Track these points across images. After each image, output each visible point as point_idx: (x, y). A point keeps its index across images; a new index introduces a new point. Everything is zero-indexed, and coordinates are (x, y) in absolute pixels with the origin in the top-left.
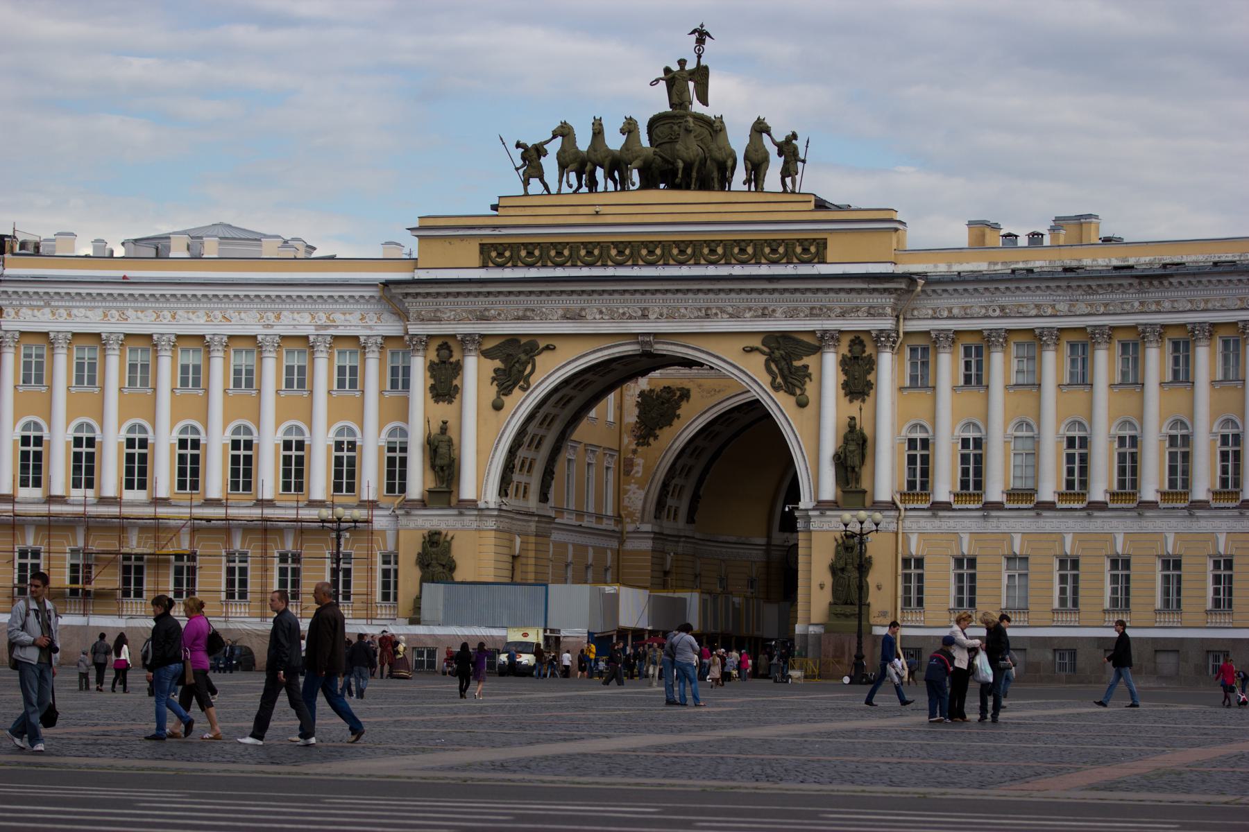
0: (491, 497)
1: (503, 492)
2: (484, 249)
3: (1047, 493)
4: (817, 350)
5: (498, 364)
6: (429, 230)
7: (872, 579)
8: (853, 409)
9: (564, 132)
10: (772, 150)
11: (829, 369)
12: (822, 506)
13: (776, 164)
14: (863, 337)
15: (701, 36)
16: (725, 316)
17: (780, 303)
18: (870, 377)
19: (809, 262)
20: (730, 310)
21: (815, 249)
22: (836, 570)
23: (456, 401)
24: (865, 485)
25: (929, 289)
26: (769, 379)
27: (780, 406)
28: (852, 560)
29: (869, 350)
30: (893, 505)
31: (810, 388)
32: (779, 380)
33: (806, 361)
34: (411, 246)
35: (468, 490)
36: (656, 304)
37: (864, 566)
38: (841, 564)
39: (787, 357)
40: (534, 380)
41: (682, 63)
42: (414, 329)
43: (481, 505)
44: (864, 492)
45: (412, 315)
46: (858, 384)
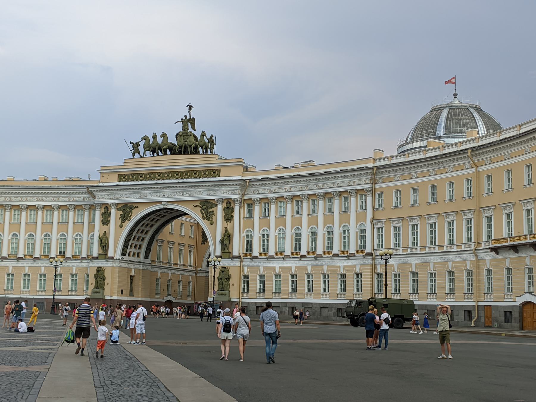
0: (118, 256)
1: (124, 254)
5: (121, 213)
6: (105, 172)
11: (219, 211)
14: (230, 201)
16: (188, 195)
18: (232, 214)
19: (215, 177)
20: (189, 193)
21: (216, 172)
25: (251, 184)
26: (202, 215)
27: (204, 224)
29: (232, 205)
30: (239, 257)
31: (214, 217)
32: (205, 216)
33: (213, 209)
34: (98, 176)
35: (110, 254)
37: (228, 278)
38: (220, 277)
42: (97, 201)
43: (115, 258)
44: (230, 253)
45: (97, 197)
46: (228, 218)
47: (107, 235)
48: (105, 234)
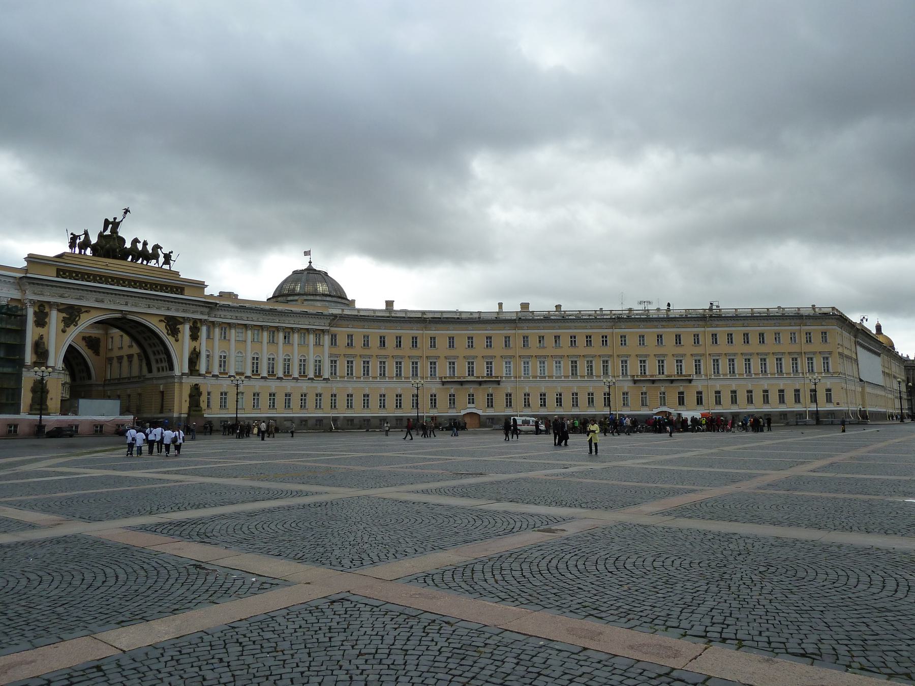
2: (58, 271)
3: (249, 373)
4: (181, 323)
7: (202, 399)
8: (194, 344)
9: (86, 233)
10: (162, 256)
11: (186, 329)
12: (183, 374)
13: (162, 259)
15: (127, 211)
17: (173, 306)
22: (191, 396)
23: (46, 327)
24: (197, 368)
27: (169, 340)
28: (195, 392)
29: (199, 325)
31: (180, 335)
35: (51, 362)
36: (131, 300)
37: (200, 394)
39: (173, 324)
40: (80, 323)
41: (115, 219)
46: (194, 337)
47: (45, 340)
48: (41, 337)
